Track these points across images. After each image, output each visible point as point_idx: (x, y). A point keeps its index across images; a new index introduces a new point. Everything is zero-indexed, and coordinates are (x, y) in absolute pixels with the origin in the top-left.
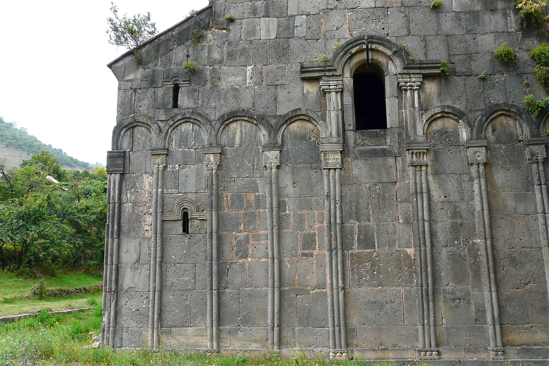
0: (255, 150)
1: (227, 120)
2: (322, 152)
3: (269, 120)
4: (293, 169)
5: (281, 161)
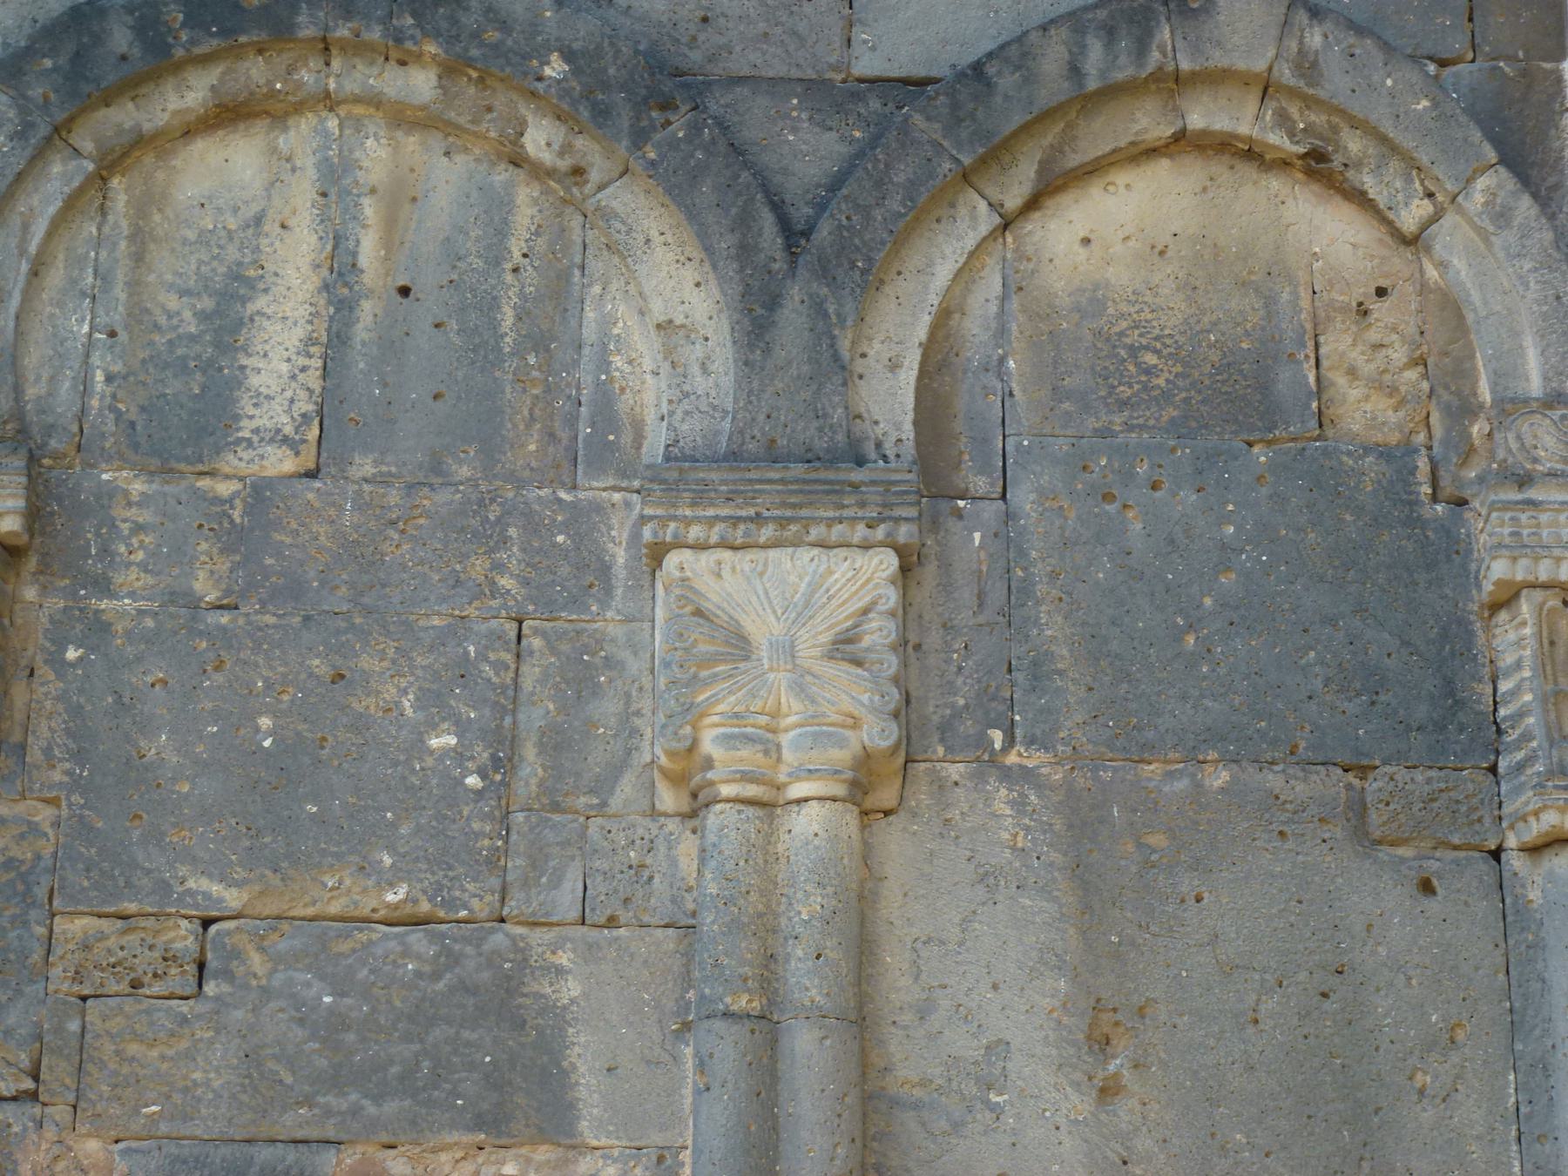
0: (533, 525)
1: (133, 84)
2: (1506, 598)
3: (750, 133)
4: (1082, 824)
5: (905, 709)
